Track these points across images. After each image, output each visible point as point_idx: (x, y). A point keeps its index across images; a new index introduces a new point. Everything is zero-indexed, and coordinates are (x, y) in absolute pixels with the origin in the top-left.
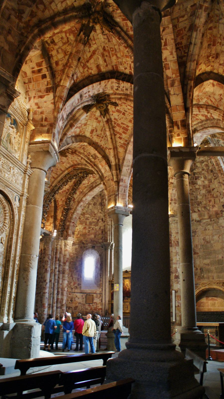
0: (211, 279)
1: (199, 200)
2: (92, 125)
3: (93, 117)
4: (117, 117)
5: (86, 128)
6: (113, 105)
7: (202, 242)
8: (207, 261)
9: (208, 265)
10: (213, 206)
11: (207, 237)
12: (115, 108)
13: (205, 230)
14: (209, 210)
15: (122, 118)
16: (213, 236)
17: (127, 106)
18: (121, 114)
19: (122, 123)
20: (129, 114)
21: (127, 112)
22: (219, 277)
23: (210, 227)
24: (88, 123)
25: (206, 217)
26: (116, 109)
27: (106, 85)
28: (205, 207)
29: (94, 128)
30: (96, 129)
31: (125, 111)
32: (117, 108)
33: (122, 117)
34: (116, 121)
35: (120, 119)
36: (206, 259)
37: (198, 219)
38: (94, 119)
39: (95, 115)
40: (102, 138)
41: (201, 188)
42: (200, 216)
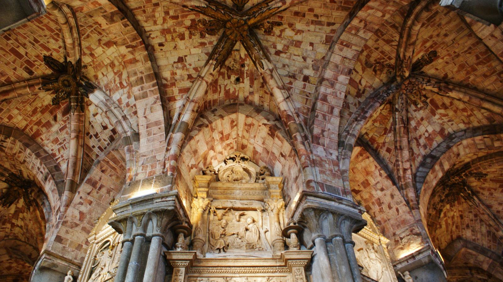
2: (104, 54)
3: (97, 61)
4: (52, 40)
5: (115, 57)
6: (55, 60)
12: (51, 54)
15: (41, 36)
17: (27, 53)
18: (41, 42)
19: (43, 30)
20: (25, 36)
21: (30, 42)
24: (109, 62)
26: (50, 53)
27: (20, 152)
29: (103, 48)
30: (100, 43)
31: (34, 45)
32: (48, 54)
33: (41, 38)
34: (55, 37)
35: (45, 36)
38: (95, 58)
39: (93, 61)
40: (91, 26)
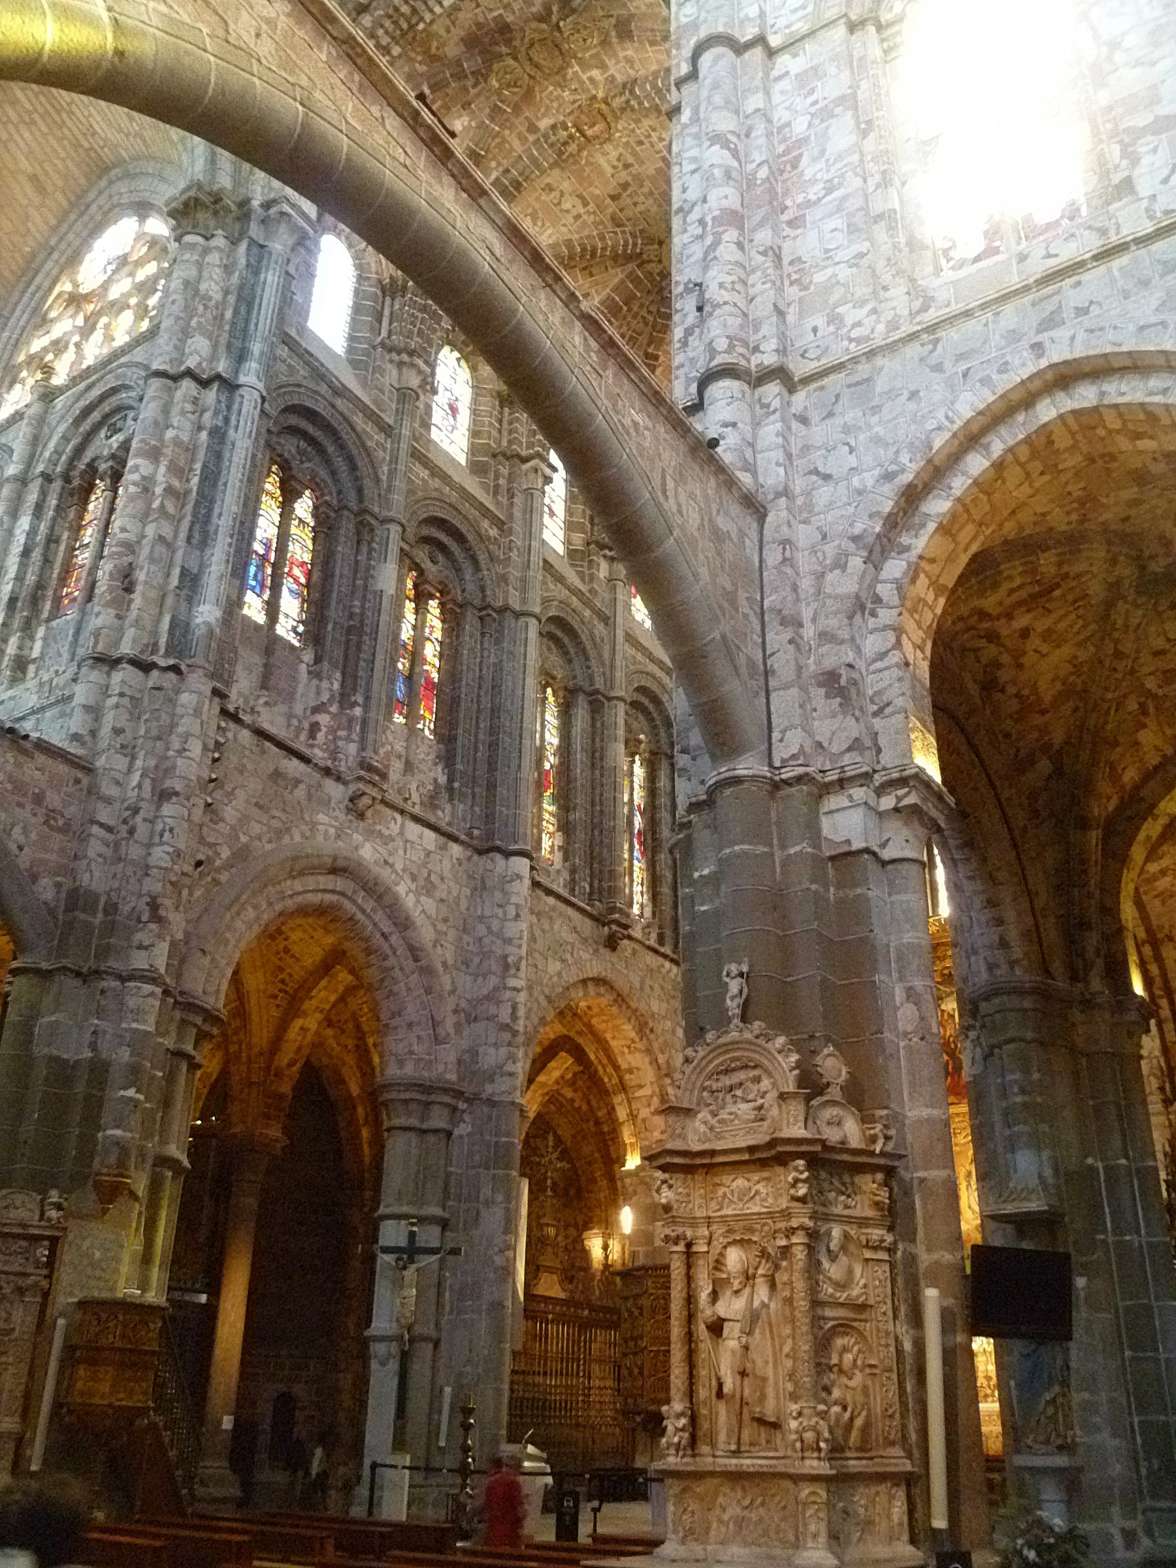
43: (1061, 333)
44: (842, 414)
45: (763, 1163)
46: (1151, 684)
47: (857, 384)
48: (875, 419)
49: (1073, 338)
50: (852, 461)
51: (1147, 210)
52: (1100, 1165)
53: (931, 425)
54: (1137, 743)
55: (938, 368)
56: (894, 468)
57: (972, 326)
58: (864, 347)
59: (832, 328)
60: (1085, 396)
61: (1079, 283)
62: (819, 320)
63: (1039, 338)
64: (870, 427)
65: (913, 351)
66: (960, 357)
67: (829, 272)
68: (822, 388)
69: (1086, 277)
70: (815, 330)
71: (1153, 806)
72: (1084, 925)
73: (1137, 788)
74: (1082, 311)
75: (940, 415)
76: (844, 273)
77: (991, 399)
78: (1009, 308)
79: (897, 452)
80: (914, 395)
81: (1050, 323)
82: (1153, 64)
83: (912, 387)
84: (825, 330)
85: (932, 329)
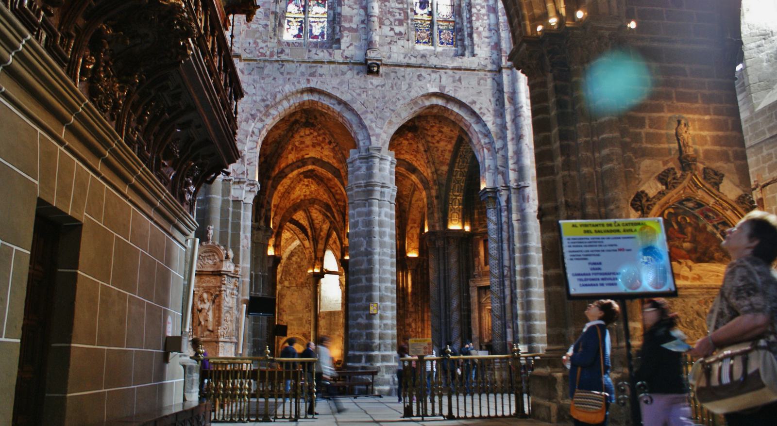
0: (293, 330)
1: (291, 272)
7: (290, 303)
8: (291, 318)
9: (292, 320)
10: (300, 278)
11: (293, 300)
13: (292, 294)
14: (297, 280)
16: (297, 300)
22: (298, 330)
23: (296, 293)
25: (294, 285)
28: (294, 278)
36: (290, 316)
37: (288, 286)
41: (294, 263)
42: (290, 283)
43: (315, 79)
44: (254, 75)
45: (215, 275)
46: (297, 144)
47: (259, 68)
48: (262, 81)
49: (317, 82)
50: (254, 91)
51: (342, 54)
52: (254, 274)
53: (277, 90)
54: (287, 158)
55: (282, 73)
56: (265, 98)
57: (293, 65)
58: (263, 58)
59: (254, 45)
60: (315, 97)
61: (322, 67)
62: (251, 41)
63: (309, 78)
64: (260, 83)
65: (276, 65)
66: (288, 73)
67: (257, 26)
68: (249, 64)
69: (324, 66)
70: (249, 43)
71: (286, 175)
72: (262, 206)
73: (284, 169)
74: (321, 75)
75: (280, 88)
76: (261, 29)
77: (294, 90)
78: (303, 65)
79: (267, 94)
80: (274, 79)
81: (313, 75)
82: (353, 9)
83: (274, 76)
84: (253, 45)
85: (282, 61)
